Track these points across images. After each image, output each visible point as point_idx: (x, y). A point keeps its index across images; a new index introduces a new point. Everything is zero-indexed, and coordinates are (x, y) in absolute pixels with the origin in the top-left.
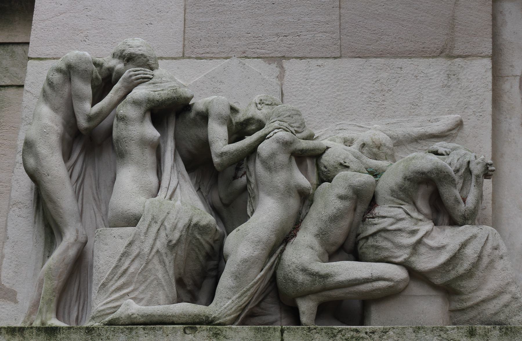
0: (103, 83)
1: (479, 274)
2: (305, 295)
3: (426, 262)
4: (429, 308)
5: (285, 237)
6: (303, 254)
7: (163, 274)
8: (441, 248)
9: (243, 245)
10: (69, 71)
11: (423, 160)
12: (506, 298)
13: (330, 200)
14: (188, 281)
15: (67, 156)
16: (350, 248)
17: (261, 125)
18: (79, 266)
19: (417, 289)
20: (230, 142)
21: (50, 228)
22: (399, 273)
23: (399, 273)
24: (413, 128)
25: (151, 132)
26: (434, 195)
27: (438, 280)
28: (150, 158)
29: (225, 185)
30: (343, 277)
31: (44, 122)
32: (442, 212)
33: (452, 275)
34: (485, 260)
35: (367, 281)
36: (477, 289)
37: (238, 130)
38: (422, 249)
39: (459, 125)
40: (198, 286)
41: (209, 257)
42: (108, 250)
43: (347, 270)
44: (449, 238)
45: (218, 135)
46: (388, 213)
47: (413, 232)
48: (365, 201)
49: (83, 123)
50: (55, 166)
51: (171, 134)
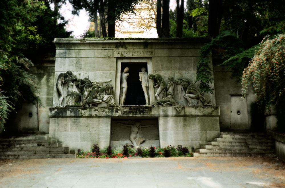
1: (110, 101)
2: (90, 103)
3: (104, 100)
8: (106, 98)
12: (113, 104)
14: (77, 101)
15: (61, 86)
16: (96, 98)
17: (85, 83)
19: (103, 102)
20: (82, 85)
22: (101, 101)
23: (101, 101)
24: (105, 81)
25: (72, 84)
27: (106, 102)
28: (72, 87)
30: (94, 101)
33: (107, 101)
34: (111, 99)
35: (98, 102)
36: (110, 103)
38: (104, 98)
39: (111, 80)
40: (78, 102)
41: (79, 99)
43: (96, 100)
47: (103, 96)
49: (63, 82)
51: (74, 83)
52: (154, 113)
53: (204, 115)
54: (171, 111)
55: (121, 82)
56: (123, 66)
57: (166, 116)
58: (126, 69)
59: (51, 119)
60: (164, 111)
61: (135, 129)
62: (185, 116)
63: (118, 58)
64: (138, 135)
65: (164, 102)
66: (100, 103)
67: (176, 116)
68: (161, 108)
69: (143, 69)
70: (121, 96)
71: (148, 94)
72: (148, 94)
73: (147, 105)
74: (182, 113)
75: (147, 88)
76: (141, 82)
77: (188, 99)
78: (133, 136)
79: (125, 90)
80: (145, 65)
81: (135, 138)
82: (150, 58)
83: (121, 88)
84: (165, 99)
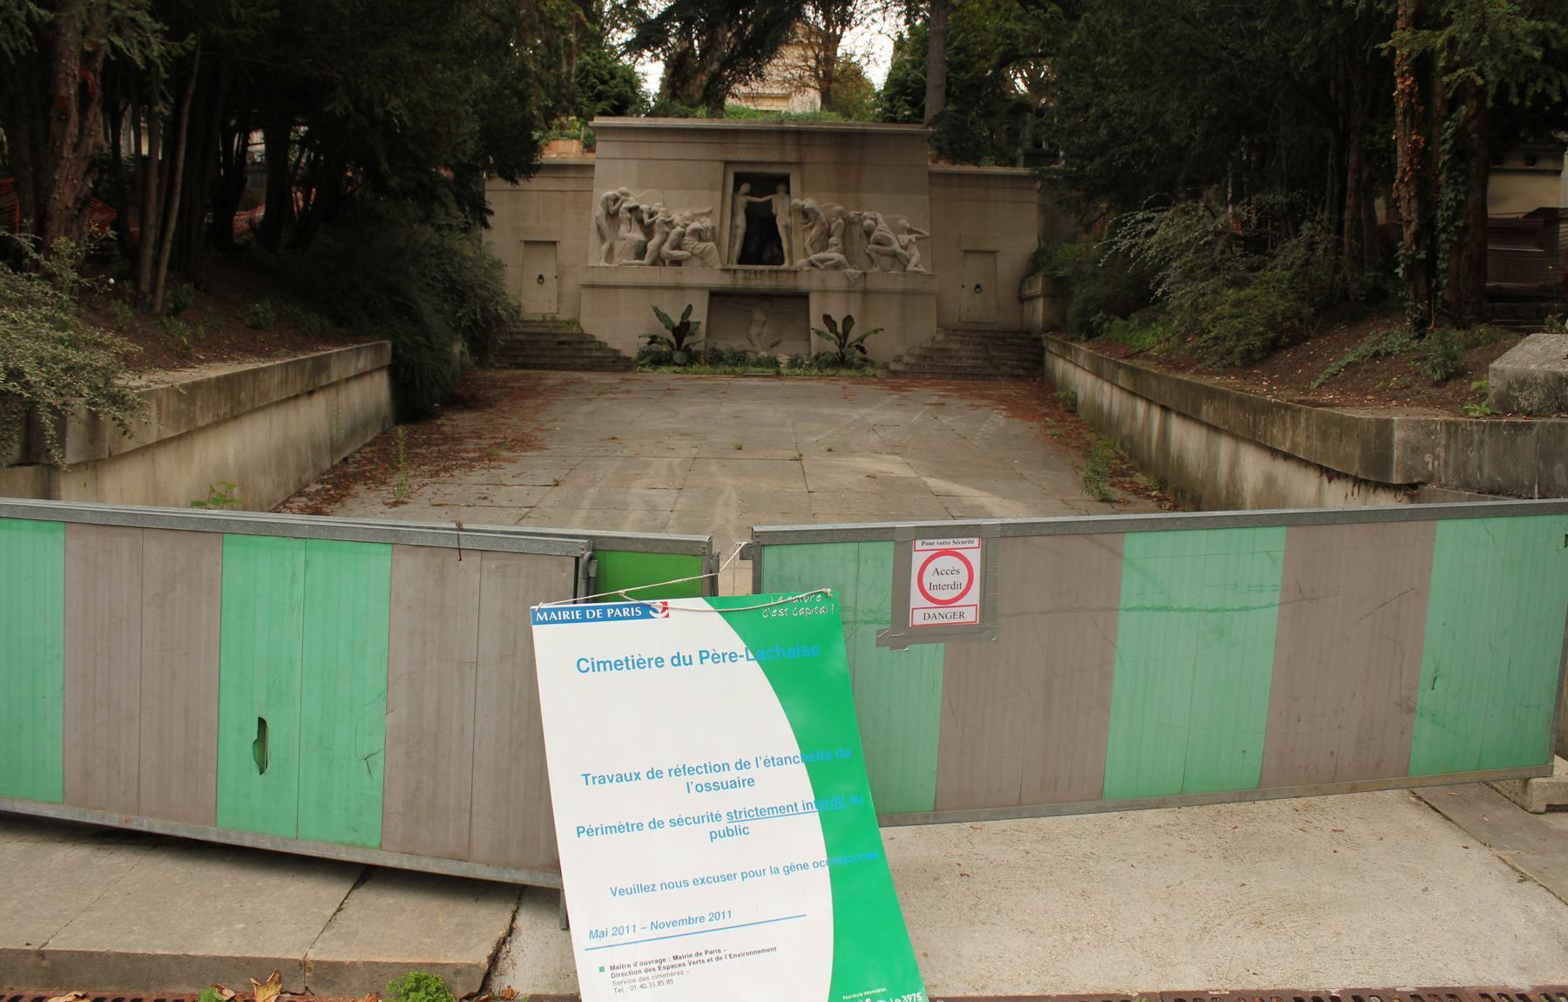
0: (616, 199)
4: (697, 262)
5: (662, 244)
6: (666, 249)
7: (633, 253)
9: (652, 245)
10: (607, 198)
11: (696, 225)
13: (673, 236)
16: (678, 246)
18: (611, 250)
21: (603, 239)
26: (698, 234)
29: (649, 231)
31: (599, 211)
32: (701, 239)
37: (651, 215)
42: (619, 245)
43: (677, 253)
44: (702, 245)
45: (645, 216)
46: (687, 239)
48: (683, 235)
50: (604, 224)
52: (803, 283)
53: (905, 293)
54: (835, 281)
55: (733, 216)
56: (739, 179)
57: (825, 291)
58: (745, 187)
59: (584, 291)
60: (823, 280)
61: (759, 315)
62: (866, 292)
63: (727, 163)
64: (766, 329)
65: (823, 261)
66: (688, 259)
67: (848, 292)
68: (817, 272)
69: (781, 187)
70: (731, 247)
71: (790, 242)
72: (790, 242)
73: (786, 265)
74: (860, 286)
75: (787, 227)
76: (774, 218)
77: (874, 255)
78: (754, 331)
79: (741, 232)
80: (785, 180)
81: (759, 335)
82: (799, 164)
83: (733, 227)
84: (822, 255)
